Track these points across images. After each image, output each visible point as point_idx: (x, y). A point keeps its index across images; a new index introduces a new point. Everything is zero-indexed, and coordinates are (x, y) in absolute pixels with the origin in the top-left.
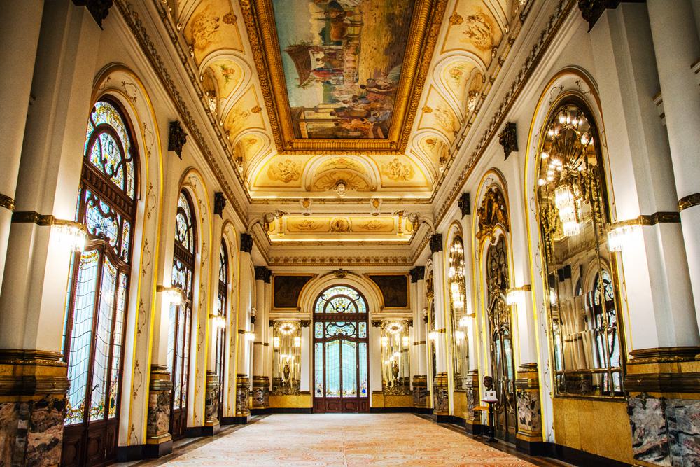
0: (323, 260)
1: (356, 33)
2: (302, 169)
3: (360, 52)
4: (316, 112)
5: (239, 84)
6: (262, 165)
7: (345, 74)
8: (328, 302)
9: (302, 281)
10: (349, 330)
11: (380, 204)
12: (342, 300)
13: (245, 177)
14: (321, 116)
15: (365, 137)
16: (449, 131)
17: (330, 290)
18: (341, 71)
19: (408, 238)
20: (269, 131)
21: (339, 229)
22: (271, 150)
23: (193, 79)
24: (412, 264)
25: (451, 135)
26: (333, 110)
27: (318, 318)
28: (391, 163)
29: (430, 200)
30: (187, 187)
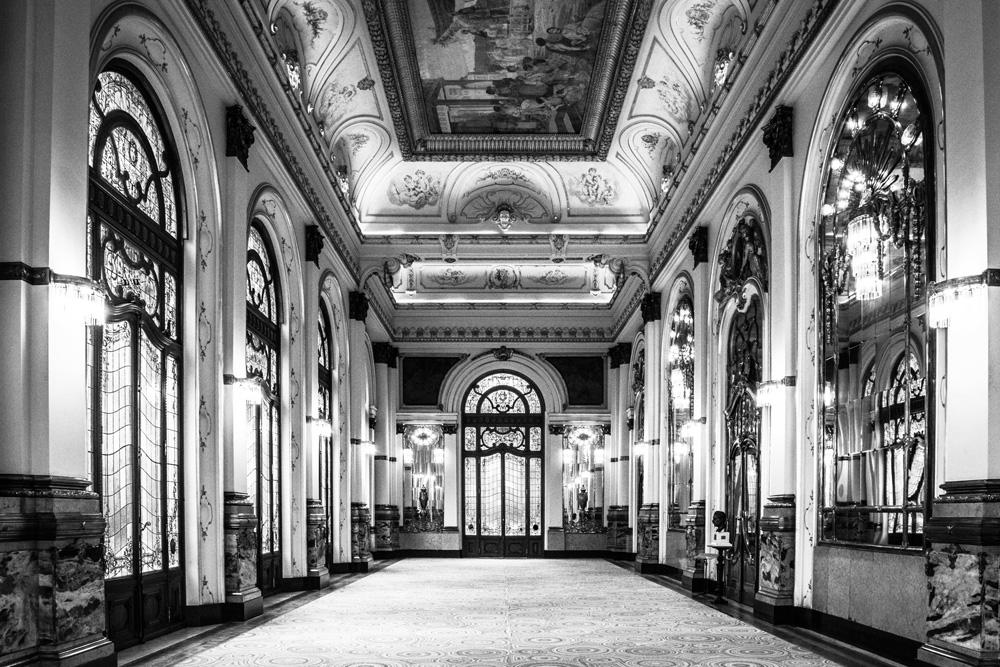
0: (475, 333)
2: (442, 186)
4: (464, 88)
5: (336, 37)
6: (380, 180)
7: (510, 19)
8: (484, 396)
9: (448, 363)
10: (516, 440)
11: (566, 244)
12: (505, 394)
13: (353, 199)
14: (472, 95)
15: (542, 131)
16: (680, 121)
17: (487, 378)
18: (505, 13)
19: (607, 299)
20: (388, 122)
21: (501, 283)
22: (392, 154)
23: (258, 30)
24: (613, 340)
25: (682, 128)
26: (490, 84)
27: (468, 420)
28: (584, 176)
29: (644, 236)
30: (260, 217)
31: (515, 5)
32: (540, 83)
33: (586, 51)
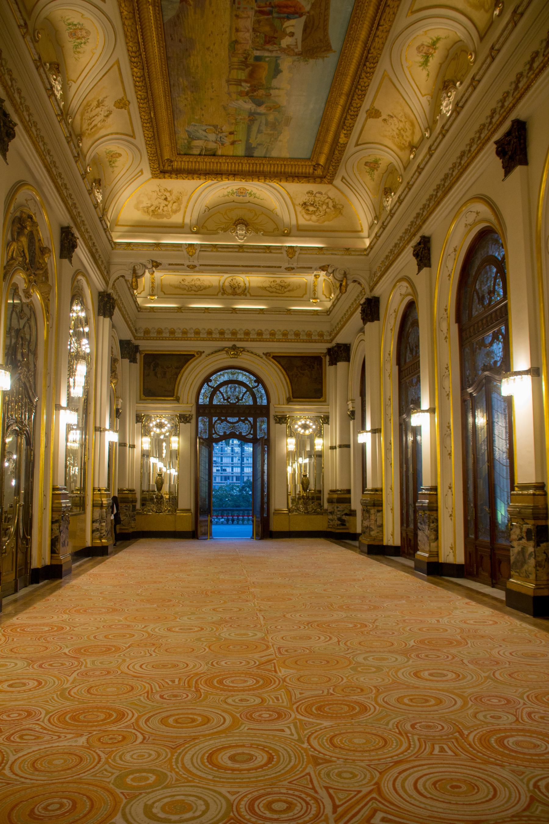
1: (235, 71)
3: (230, 45)
31: (249, 20)
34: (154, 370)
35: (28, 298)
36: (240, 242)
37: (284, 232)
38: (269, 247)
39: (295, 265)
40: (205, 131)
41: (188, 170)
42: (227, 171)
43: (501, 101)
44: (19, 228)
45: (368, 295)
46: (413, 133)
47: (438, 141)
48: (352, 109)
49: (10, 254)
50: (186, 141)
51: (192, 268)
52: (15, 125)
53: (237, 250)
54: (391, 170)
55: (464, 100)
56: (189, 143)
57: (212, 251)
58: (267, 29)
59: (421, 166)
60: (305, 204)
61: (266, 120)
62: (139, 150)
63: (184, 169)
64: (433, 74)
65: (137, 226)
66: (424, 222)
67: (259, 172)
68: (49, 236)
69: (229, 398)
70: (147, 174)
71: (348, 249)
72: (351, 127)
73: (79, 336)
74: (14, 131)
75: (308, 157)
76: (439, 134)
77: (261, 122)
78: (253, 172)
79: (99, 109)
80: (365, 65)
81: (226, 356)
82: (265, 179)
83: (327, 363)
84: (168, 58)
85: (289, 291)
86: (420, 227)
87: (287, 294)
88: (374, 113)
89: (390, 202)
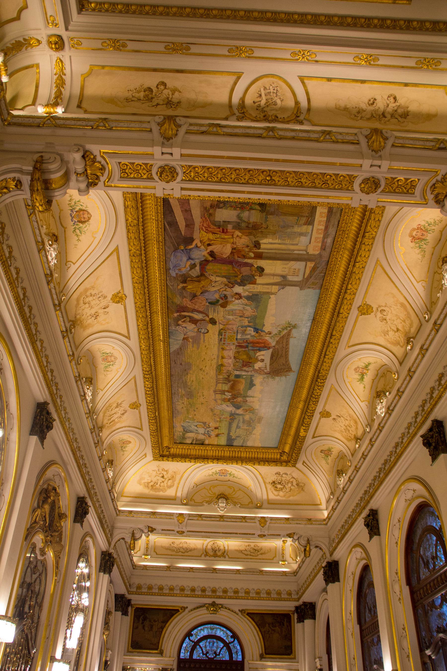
3: (217, 367)
4: (284, 277)
7: (235, 342)
26: (259, 280)
31: (231, 351)
32: (213, 278)
33: (178, 311)
34: (142, 623)
35: (43, 555)
36: (221, 513)
37: (257, 505)
38: (244, 518)
39: (266, 533)
40: (196, 426)
41: (181, 455)
42: (213, 456)
43: (421, 406)
44: (44, 498)
45: (329, 559)
46: (357, 428)
47: (377, 434)
48: (309, 411)
49: (34, 518)
50: (181, 433)
51: (181, 533)
52: (54, 420)
53: (218, 519)
54: (341, 456)
55: (393, 405)
56: (184, 435)
57: (198, 520)
58: (244, 357)
59: (365, 454)
60: (274, 482)
61: (243, 419)
62: (145, 440)
63: (179, 454)
64: (368, 387)
65: (138, 497)
66: (371, 497)
67: (238, 457)
68: (67, 504)
69: (207, 653)
70: (150, 457)
71: (310, 520)
72: (309, 425)
73: (81, 589)
74: (52, 425)
75: (276, 446)
76: (377, 430)
77: (239, 420)
78: (232, 457)
79: (117, 409)
80: (317, 381)
81: (206, 612)
82: (242, 463)
83: (296, 621)
84: (171, 375)
85: (261, 554)
86: (368, 502)
87: (260, 557)
88: (326, 414)
89: (342, 481)
